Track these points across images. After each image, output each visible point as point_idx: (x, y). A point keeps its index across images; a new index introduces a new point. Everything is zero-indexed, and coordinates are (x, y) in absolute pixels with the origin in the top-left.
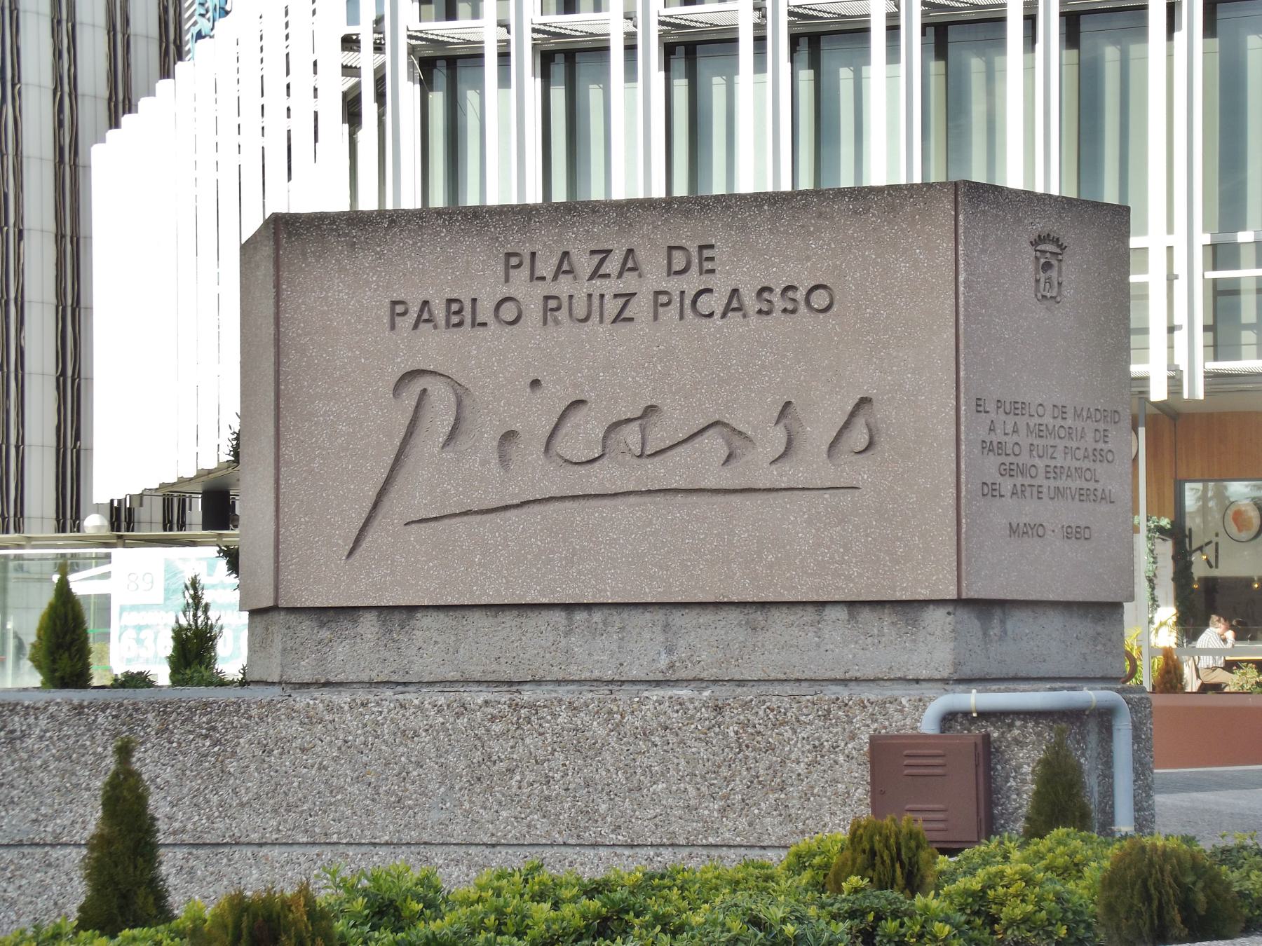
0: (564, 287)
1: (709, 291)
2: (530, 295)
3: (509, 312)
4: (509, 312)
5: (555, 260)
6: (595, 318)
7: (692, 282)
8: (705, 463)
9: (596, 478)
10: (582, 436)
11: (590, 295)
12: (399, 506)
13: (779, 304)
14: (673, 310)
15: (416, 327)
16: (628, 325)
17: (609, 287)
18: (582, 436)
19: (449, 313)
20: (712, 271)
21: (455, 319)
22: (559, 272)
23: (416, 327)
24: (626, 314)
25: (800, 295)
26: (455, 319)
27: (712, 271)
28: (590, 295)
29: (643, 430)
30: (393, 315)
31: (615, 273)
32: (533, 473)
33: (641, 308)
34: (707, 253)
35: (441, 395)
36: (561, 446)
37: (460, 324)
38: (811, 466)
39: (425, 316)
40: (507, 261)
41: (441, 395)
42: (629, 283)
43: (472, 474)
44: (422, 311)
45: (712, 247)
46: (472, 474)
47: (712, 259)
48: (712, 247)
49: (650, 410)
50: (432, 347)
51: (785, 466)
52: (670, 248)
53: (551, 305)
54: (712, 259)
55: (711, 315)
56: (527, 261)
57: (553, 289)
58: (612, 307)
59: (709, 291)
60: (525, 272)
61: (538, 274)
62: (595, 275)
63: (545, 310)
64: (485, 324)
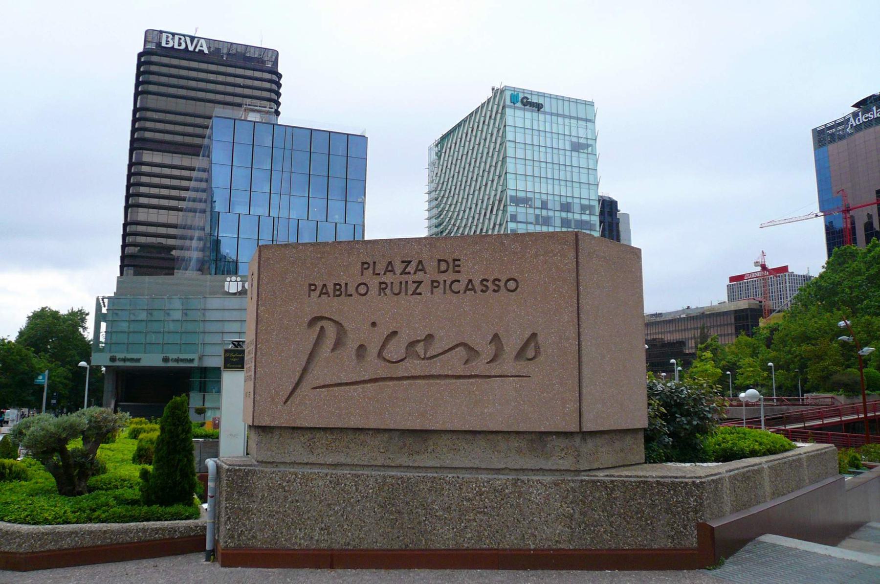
0: (388, 278)
1: (459, 281)
2: (374, 283)
3: (362, 289)
4: (362, 289)
5: (385, 265)
6: (403, 293)
7: (450, 277)
8: (455, 363)
9: (400, 370)
10: (395, 350)
11: (401, 283)
12: (312, 379)
13: (489, 284)
14: (440, 290)
15: (320, 296)
16: (419, 297)
17: (410, 278)
18: (395, 350)
19: (335, 290)
20: (459, 272)
21: (338, 293)
22: (387, 271)
23: (320, 296)
24: (418, 291)
25: (502, 284)
26: (338, 293)
27: (459, 272)
28: (401, 283)
29: (425, 345)
30: (310, 290)
31: (412, 272)
32: (373, 367)
33: (424, 289)
34: (456, 263)
35: (331, 331)
36: (387, 354)
37: (339, 296)
38: (508, 365)
39: (324, 292)
40: (432, 284)
41: (331, 331)
42: (420, 276)
43: (345, 366)
44: (322, 289)
45: (459, 260)
46: (345, 366)
47: (459, 266)
48: (459, 260)
49: (430, 337)
50: (330, 306)
51: (493, 365)
52: (440, 261)
53: (383, 287)
54: (459, 266)
55: (459, 292)
56: (372, 266)
57: (383, 279)
58: (412, 287)
59: (459, 281)
60: (371, 270)
61: (377, 272)
62: (404, 272)
63: (380, 288)
64: (351, 295)
